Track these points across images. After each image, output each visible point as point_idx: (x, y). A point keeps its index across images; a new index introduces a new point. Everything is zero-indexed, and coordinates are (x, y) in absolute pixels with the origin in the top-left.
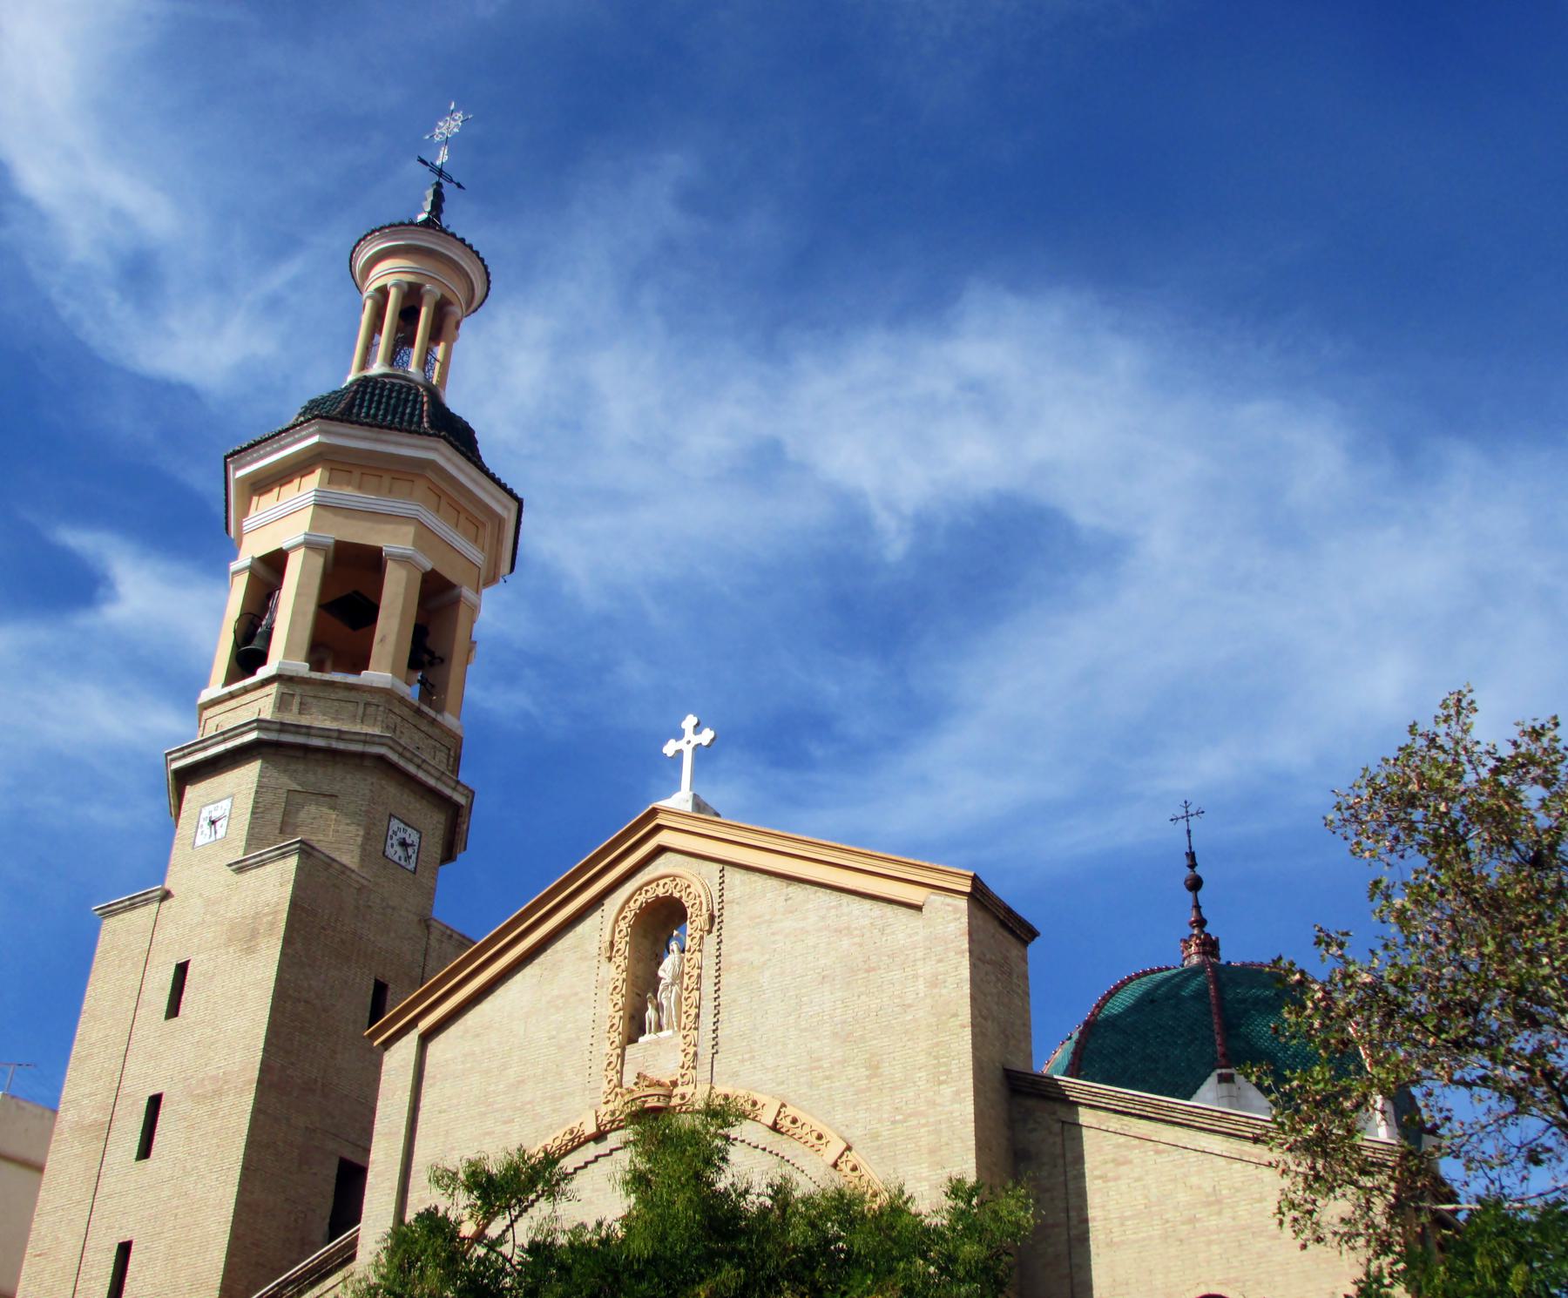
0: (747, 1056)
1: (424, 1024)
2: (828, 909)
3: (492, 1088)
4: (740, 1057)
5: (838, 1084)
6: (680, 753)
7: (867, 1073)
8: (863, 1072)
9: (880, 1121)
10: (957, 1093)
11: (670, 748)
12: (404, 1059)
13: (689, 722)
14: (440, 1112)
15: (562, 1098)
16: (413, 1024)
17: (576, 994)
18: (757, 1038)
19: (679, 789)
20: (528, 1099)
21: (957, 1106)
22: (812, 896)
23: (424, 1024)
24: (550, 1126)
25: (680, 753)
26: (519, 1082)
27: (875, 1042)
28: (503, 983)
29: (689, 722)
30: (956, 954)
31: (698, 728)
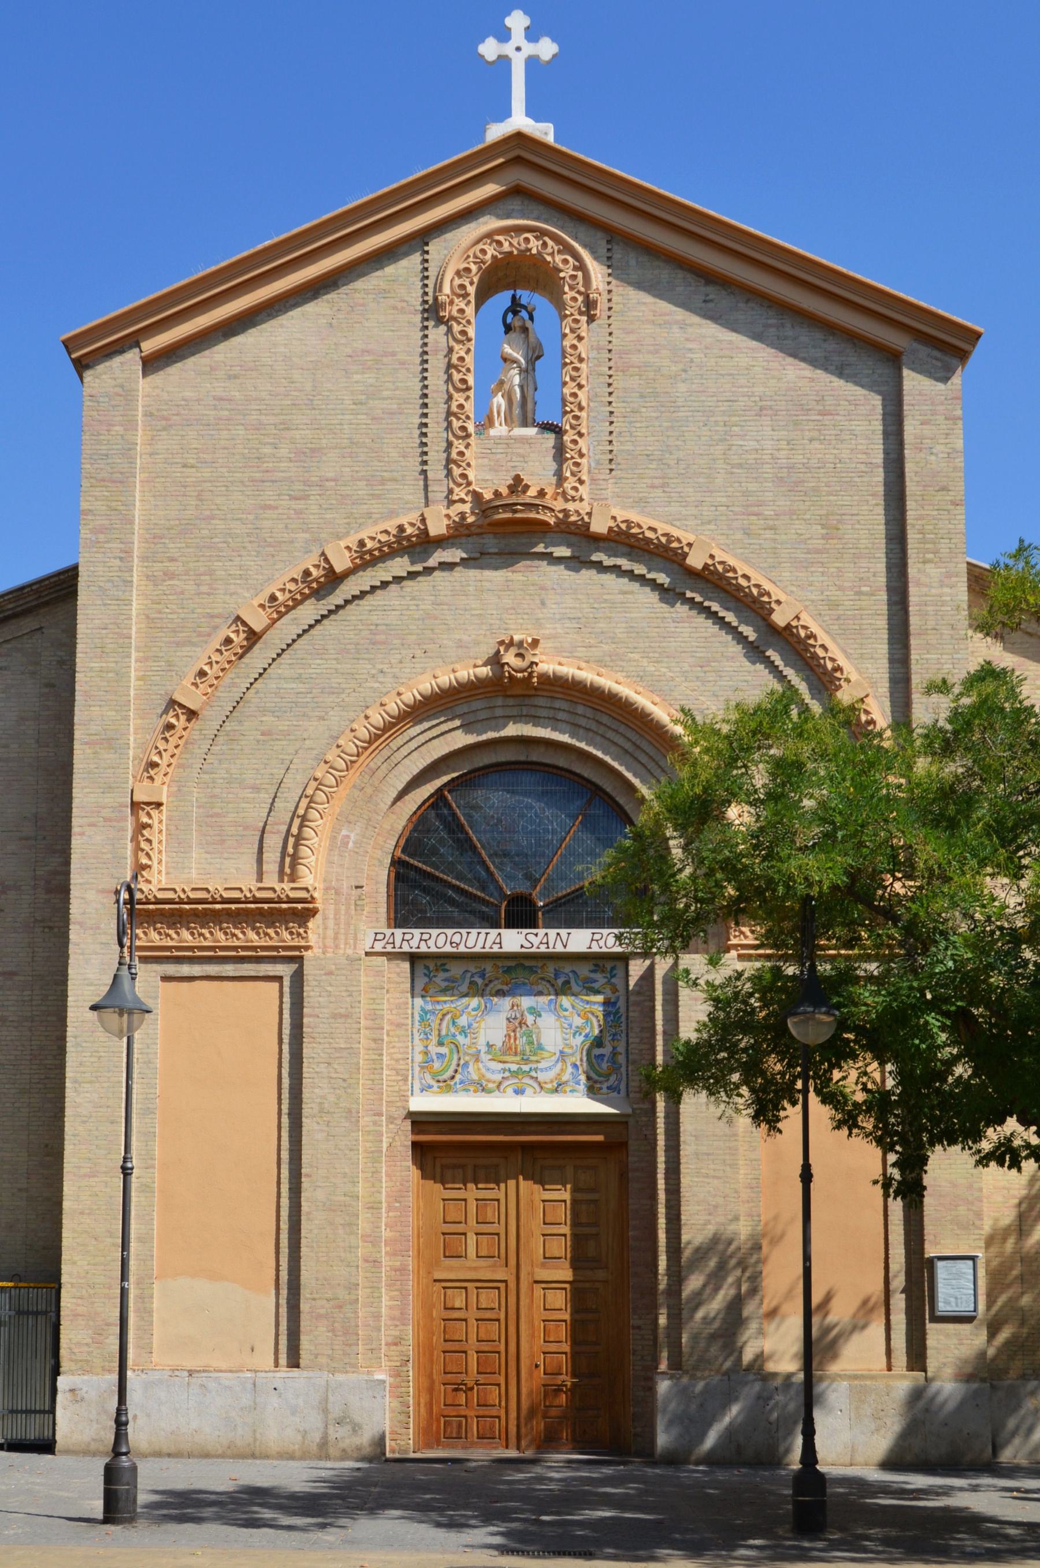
0: (657, 482)
1: (151, 345)
2: (767, 326)
3: (267, 450)
4: (649, 481)
5: (784, 537)
6: (504, 61)
7: (824, 531)
8: (819, 530)
9: (841, 588)
10: (948, 575)
11: (489, 49)
12: (122, 386)
13: (517, 21)
14: (185, 466)
15: (383, 482)
16: (133, 341)
17: (394, 354)
18: (672, 463)
19: (509, 115)
20: (331, 475)
21: (946, 590)
22: (741, 305)
23: (151, 345)
24: (369, 515)
25: (504, 61)
26: (313, 450)
27: (831, 498)
28: (271, 316)
29: (517, 21)
30: (946, 419)
31: (532, 35)
